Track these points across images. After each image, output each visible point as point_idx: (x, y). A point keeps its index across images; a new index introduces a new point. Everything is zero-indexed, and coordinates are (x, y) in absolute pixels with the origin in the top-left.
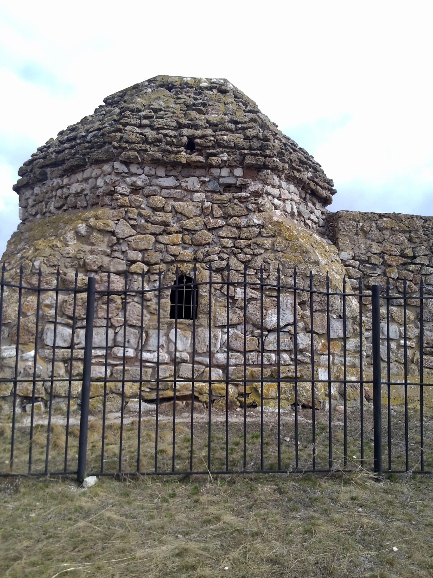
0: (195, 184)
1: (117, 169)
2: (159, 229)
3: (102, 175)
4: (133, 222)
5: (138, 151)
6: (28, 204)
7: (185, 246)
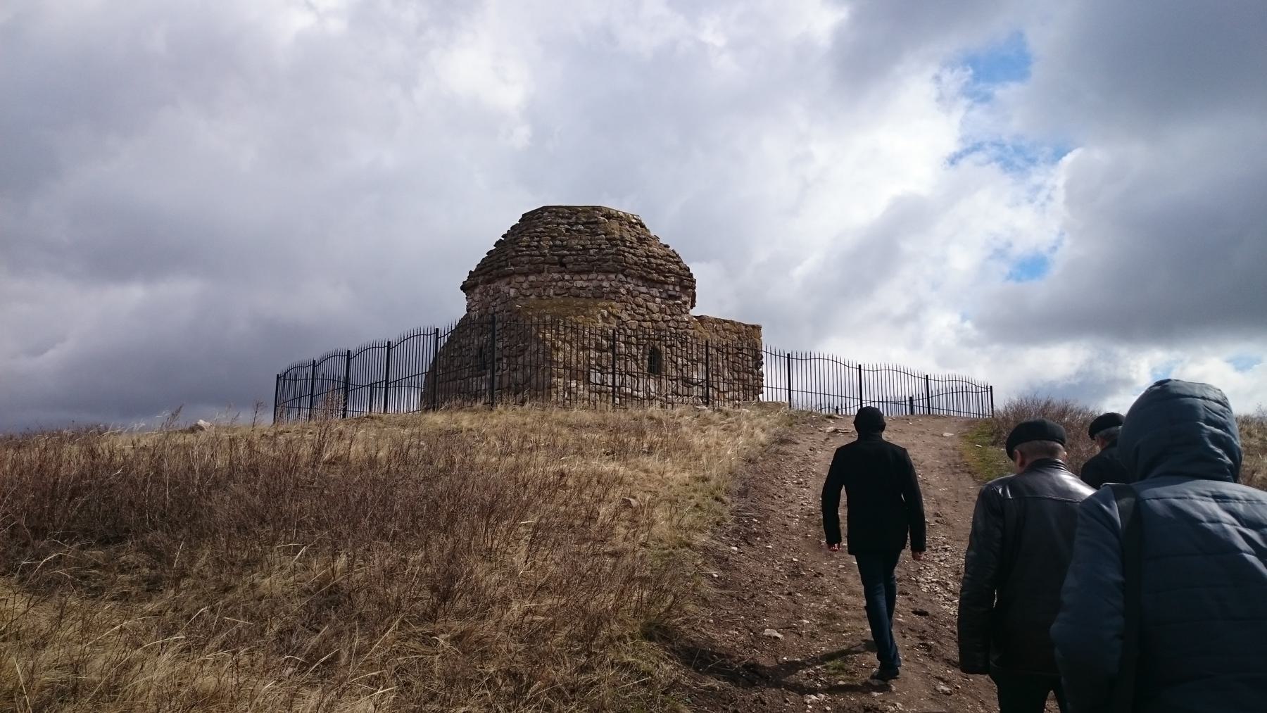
2: (640, 318)
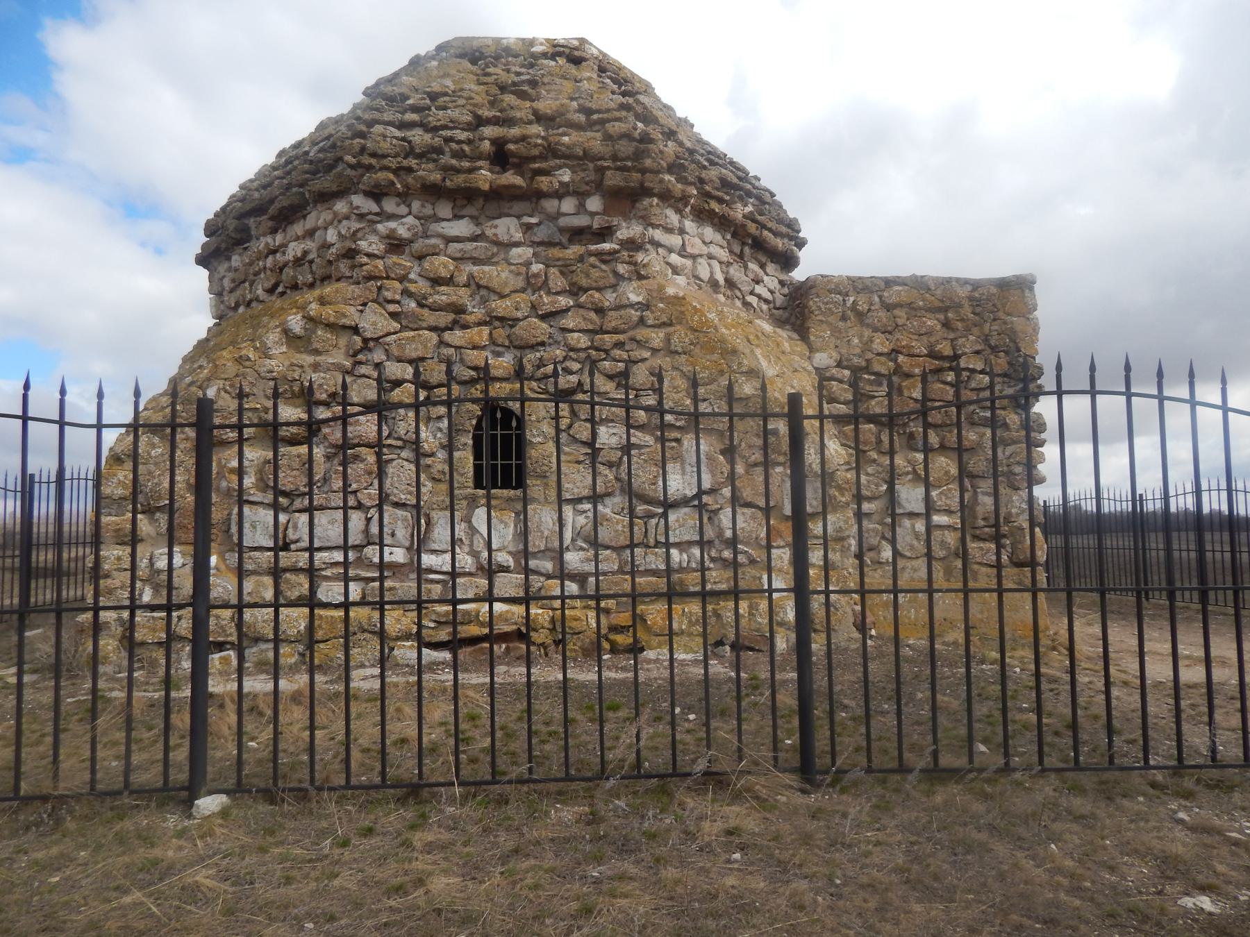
0: (512, 231)
1: (358, 208)
2: (445, 318)
3: (336, 222)
4: (392, 308)
5: (396, 171)
6: (222, 286)
7: (498, 349)
